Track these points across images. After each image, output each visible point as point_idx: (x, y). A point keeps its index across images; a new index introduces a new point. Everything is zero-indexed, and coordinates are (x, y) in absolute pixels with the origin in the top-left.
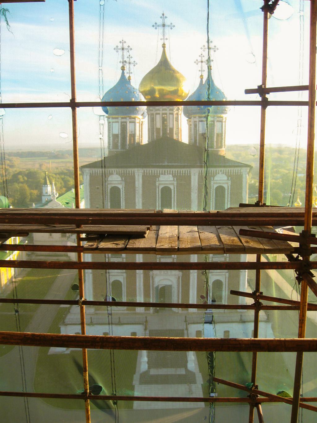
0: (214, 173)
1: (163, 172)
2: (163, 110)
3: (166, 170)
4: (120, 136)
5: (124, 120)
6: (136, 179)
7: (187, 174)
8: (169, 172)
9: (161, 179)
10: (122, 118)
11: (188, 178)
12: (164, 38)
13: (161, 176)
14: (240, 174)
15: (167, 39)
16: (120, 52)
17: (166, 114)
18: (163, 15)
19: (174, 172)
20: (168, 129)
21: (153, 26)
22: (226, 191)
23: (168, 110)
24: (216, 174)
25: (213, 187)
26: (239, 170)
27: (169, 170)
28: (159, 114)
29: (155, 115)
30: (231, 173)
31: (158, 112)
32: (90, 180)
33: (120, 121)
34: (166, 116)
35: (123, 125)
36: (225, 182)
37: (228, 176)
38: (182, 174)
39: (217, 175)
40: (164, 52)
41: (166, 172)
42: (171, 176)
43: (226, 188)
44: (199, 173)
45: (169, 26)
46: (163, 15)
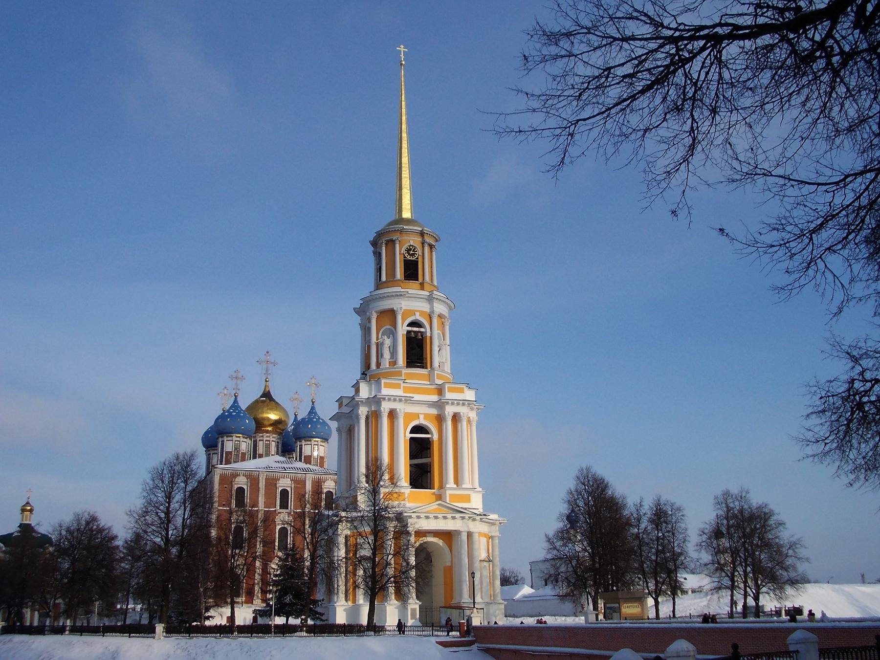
2: (267, 437)
6: (260, 481)
9: (280, 482)
10: (237, 437)
12: (267, 373)
15: (270, 374)
16: (234, 381)
17: (269, 441)
18: (268, 352)
21: (258, 362)
28: (263, 440)
31: (261, 439)
32: (220, 479)
39: (327, 481)
45: (272, 363)
46: (268, 352)
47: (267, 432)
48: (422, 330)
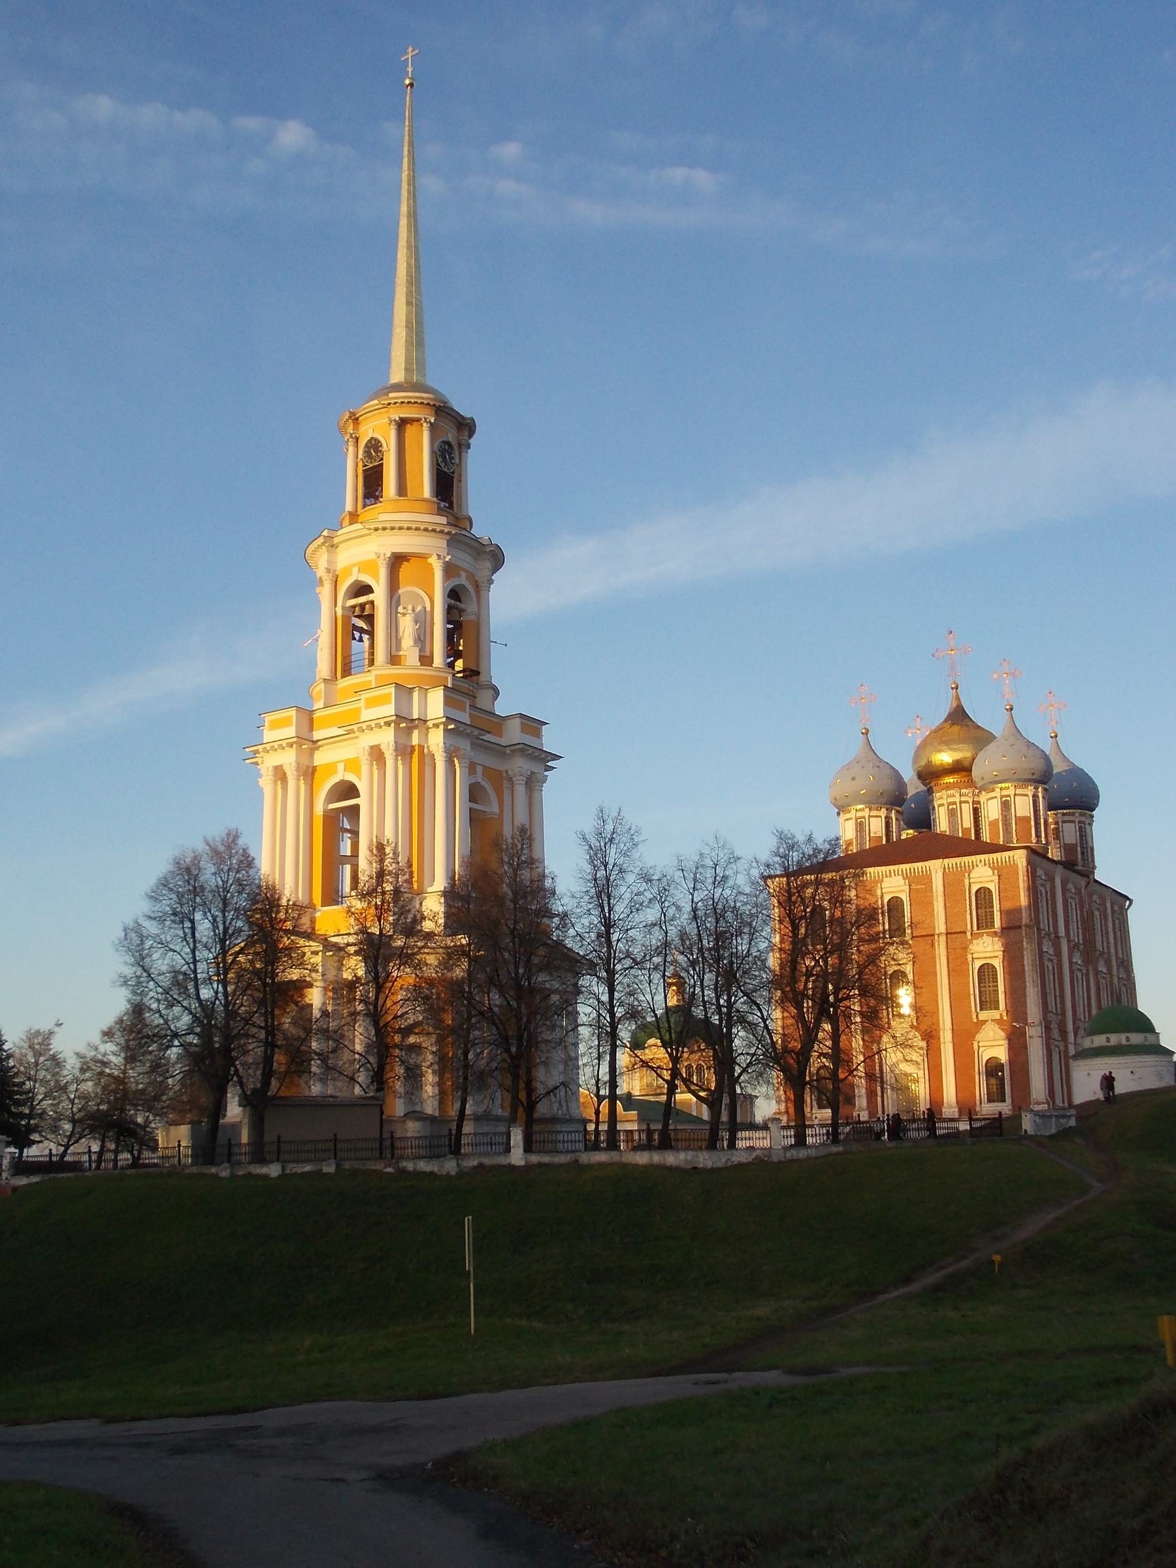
0: (969, 866)
1: (888, 873)
3: (892, 868)
4: (854, 841)
5: (859, 814)
7: (926, 871)
8: (896, 873)
11: (927, 879)
13: (885, 879)
14: (1014, 863)
17: (955, 803)
19: (904, 872)
20: (960, 831)
21: (933, 655)
22: (994, 894)
23: (958, 795)
24: (973, 868)
25: (969, 890)
26: (1011, 856)
27: (895, 867)
28: (942, 805)
29: (936, 808)
30: (997, 862)
31: (940, 802)
33: (853, 816)
34: (954, 806)
35: (861, 823)
36: (990, 879)
37: (993, 869)
38: (918, 872)
39: (976, 869)
40: (958, 698)
41: (892, 872)
42: (901, 877)
43: (993, 891)
44: (944, 868)
47: (949, 787)
48: (370, 597)
